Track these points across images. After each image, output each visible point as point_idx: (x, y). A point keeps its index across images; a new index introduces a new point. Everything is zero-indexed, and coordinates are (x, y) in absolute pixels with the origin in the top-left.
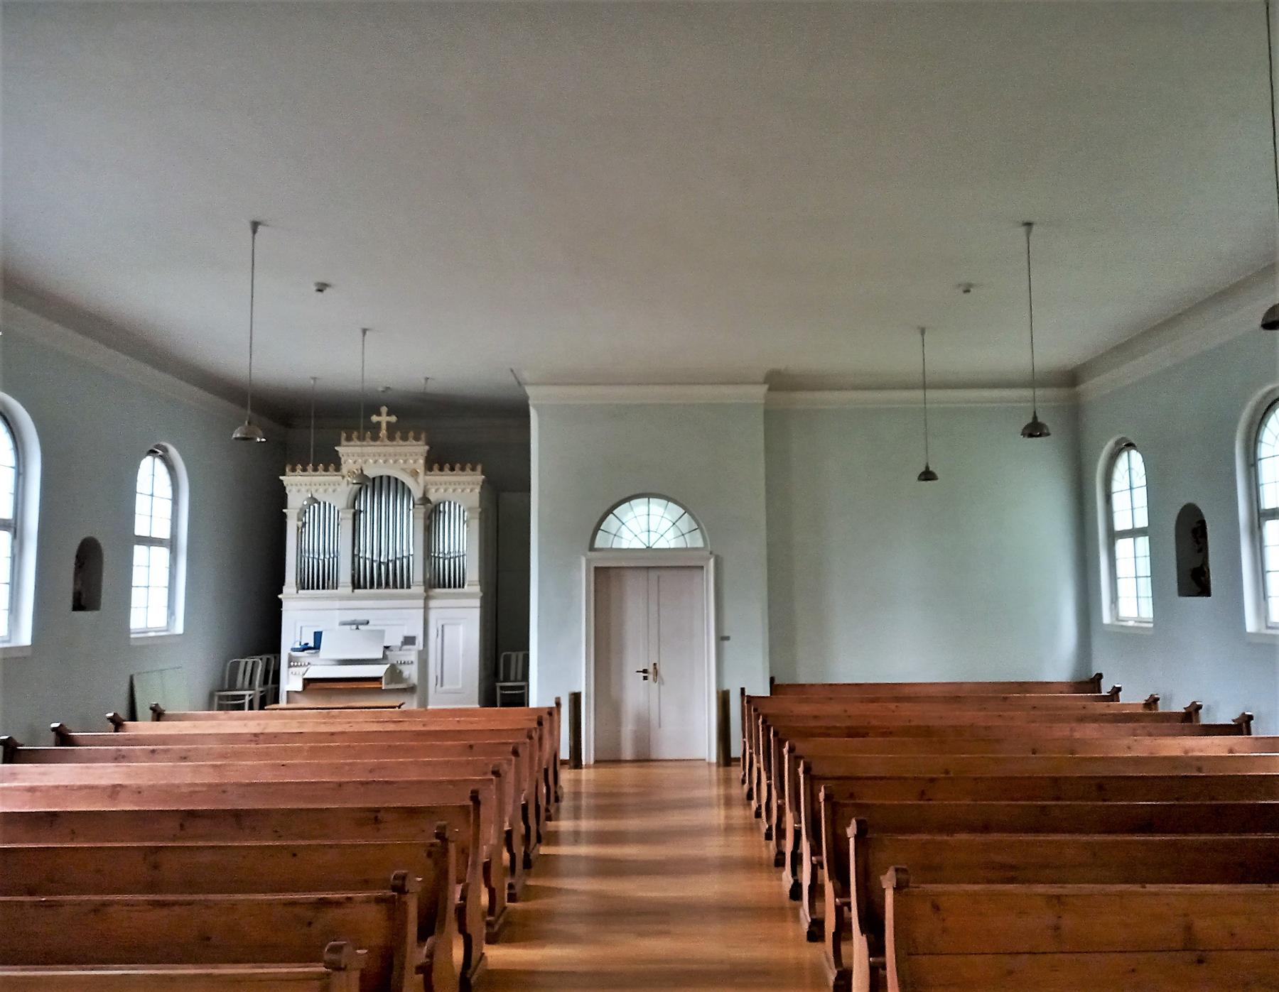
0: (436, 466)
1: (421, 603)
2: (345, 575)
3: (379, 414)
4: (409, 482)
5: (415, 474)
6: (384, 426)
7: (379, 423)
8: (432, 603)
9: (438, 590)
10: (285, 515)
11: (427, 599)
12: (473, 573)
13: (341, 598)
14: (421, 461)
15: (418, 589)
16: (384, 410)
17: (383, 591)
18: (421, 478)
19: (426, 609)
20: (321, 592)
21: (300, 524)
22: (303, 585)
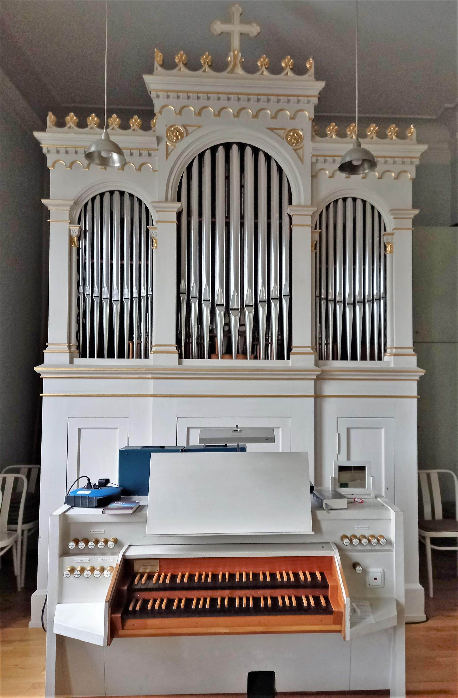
0: (332, 128)
1: (309, 387)
2: (163, 327)
3: (228, 20)
4: (282, 155)
5: (294, 141)
6: (236, 43)
7: (227, 35)
8: (330, 388)
9: (339, 364)
10: (44, 213)
11: (320, 379)
12: (400, 332)
13: (161, 374)
14: (308, 114)
15: (302, 359)
16: (237, 10)
17: (234, 363)
18: (309, 146)
19: (318, 397)
20: (116, 361)
21: (75, 229)
22: (87, 346)
